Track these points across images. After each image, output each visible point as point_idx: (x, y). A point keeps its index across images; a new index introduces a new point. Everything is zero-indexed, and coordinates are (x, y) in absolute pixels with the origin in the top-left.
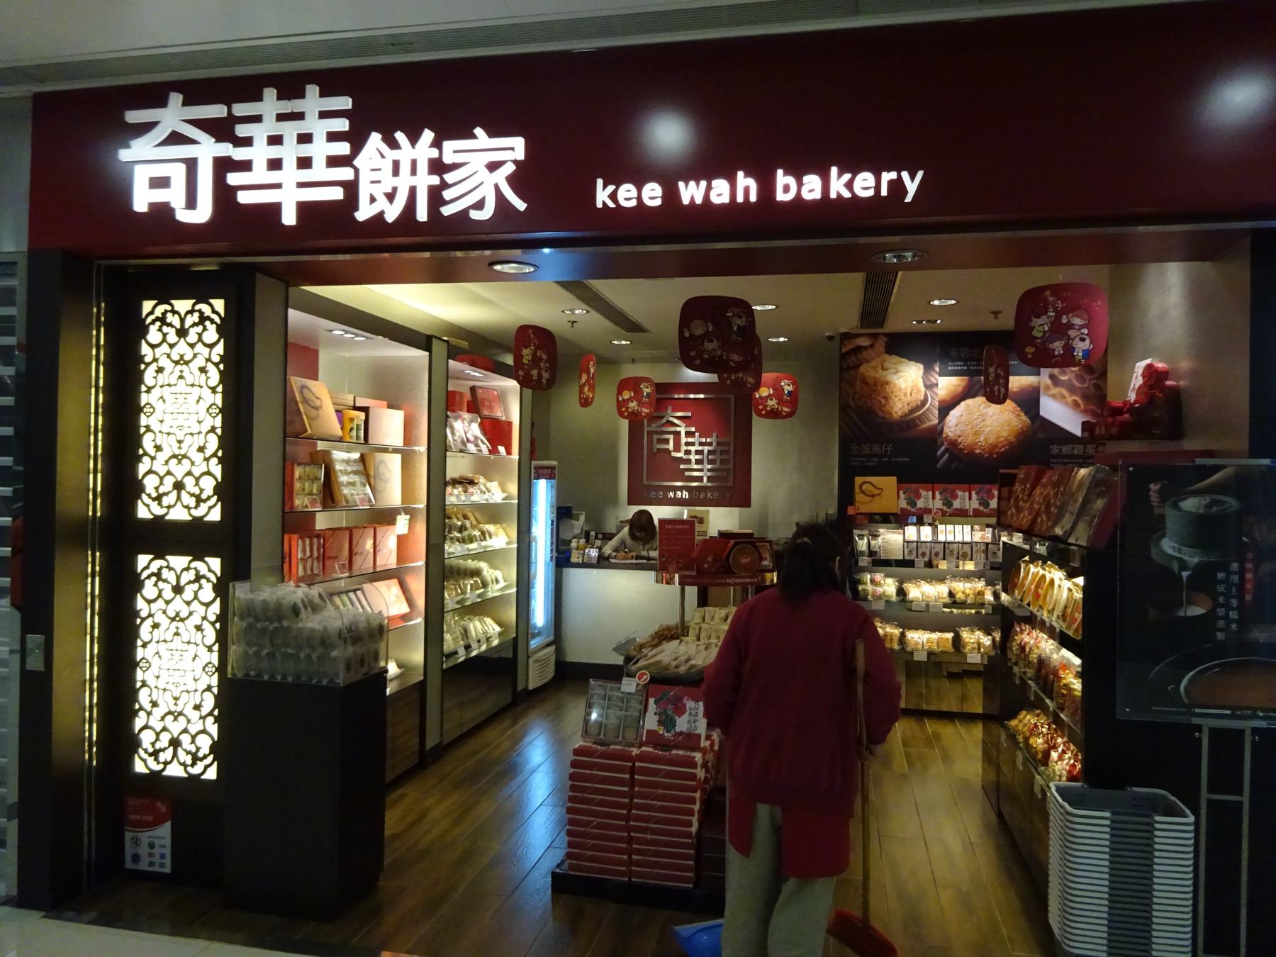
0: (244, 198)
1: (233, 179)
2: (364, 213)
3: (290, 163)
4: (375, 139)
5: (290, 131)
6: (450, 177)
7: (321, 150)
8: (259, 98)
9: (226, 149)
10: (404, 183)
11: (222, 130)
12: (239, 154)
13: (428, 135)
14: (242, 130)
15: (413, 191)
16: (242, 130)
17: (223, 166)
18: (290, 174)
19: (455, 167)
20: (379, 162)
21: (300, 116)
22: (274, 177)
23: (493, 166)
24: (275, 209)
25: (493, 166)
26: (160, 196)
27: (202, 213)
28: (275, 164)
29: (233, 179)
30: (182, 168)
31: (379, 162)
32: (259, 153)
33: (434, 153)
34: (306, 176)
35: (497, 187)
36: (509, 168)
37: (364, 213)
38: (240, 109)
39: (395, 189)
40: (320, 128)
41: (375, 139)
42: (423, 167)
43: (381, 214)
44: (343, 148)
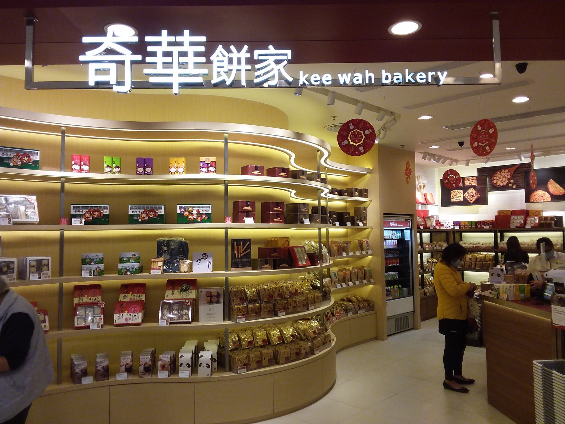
5: (176, 50)
8: (159, 34)
9: (139, 57)
14: (150, 49)
16: (150, 49)
21: (181, 44)
35: (279, 70)
38: (148, 39)
40: (191, 50)
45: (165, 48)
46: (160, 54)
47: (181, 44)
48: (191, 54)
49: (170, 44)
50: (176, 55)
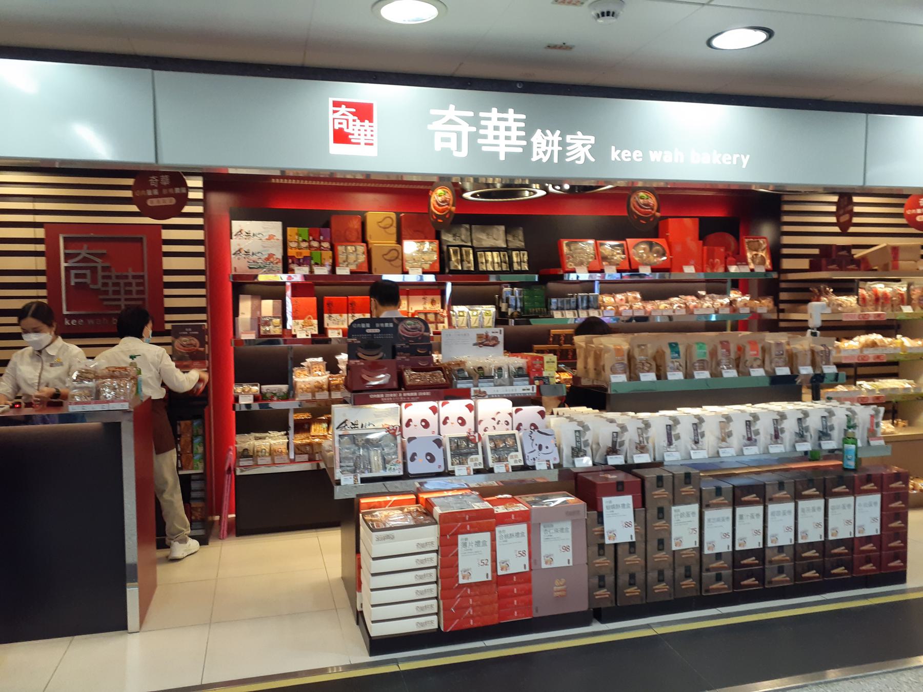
0: (484, 149)
1: (480, 141)
2: (535, 158)
3: (502, 138)
4: (539, 131)
5: (502, 125)
6: (569, 148)
7: (514, 133)
8: (490, 111)
10: (550, 149)
11: (475, 121)
12: (482, 132)
13: (558, 132)
14: (483, 123)
15: (552, 151)
17: (473, 137)
18: (502, 142)
19: (570, 144)
20: (540, 140)
21: (506, 120)
22: (495, 142)
23: (584, 145)
24: (496, 154)
25: (584, 145)
26: (446, 145)
27: (464, 153)
28: (496, 137)
29: (480, 141)
30: (455, 135)
31: (540, 140)
32: (490, 132)
33: (561, 139)
34: (508, 142)
36: (590, 146)
37: (535, 158)
39: (547, 151)
41: (539, 131)
42: (556, 143)
43: (541, 159)
44: (523, 133)
45: (494, 122)
46: (491, 128)
47: (506, 120)
48: (514, 129)
49: (499, 119)
50: (502, 128)
